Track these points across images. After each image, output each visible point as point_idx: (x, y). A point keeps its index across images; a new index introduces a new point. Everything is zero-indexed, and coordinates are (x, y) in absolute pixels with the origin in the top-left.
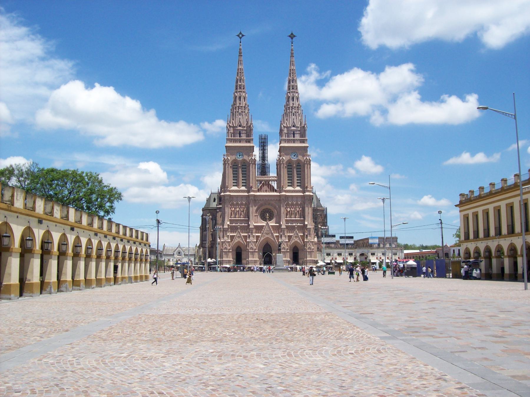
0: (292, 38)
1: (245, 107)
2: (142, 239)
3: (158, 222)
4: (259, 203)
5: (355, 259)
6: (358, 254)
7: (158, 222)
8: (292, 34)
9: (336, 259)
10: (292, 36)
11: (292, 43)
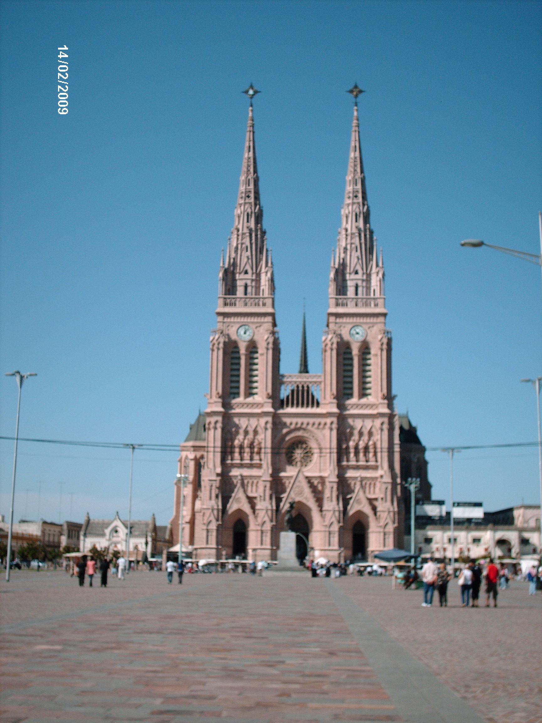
0: (356, 96)
8: (356, 87)
9: (445, 550)
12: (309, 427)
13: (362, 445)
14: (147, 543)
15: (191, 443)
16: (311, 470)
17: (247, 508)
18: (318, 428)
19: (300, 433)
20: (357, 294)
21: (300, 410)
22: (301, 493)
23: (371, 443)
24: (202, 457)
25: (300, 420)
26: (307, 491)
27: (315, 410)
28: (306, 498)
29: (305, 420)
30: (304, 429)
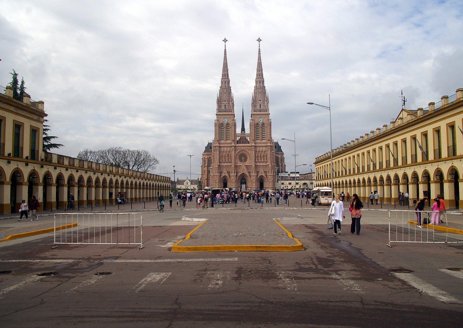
0: (259, 42)
1: (228, 89)
2: (168, 180)
3: (174, 171)
4: (238, 150)
5: (300, 186)
6: (302, 184)
7: (174, 171)
8: (259, 39)
9: (288, 186)
10: (259, 40)
11: (259, 45)
12: (246, 150)
13: (262, 155)
14: (197, 187)
15: (206, 153)
16: (247, 163)
17: (227, 175)
18: (248, 150)
19: (243, 152)
20: (260, 108)
21: (243, 145)
22: (244, 170)
23: (265, 155)
24: (210, 158)
25: (243, 148)
26: (246, 170)
27: (249, 145)
28: (246, 172)
29: (245, 148)
30: (245, 151)
